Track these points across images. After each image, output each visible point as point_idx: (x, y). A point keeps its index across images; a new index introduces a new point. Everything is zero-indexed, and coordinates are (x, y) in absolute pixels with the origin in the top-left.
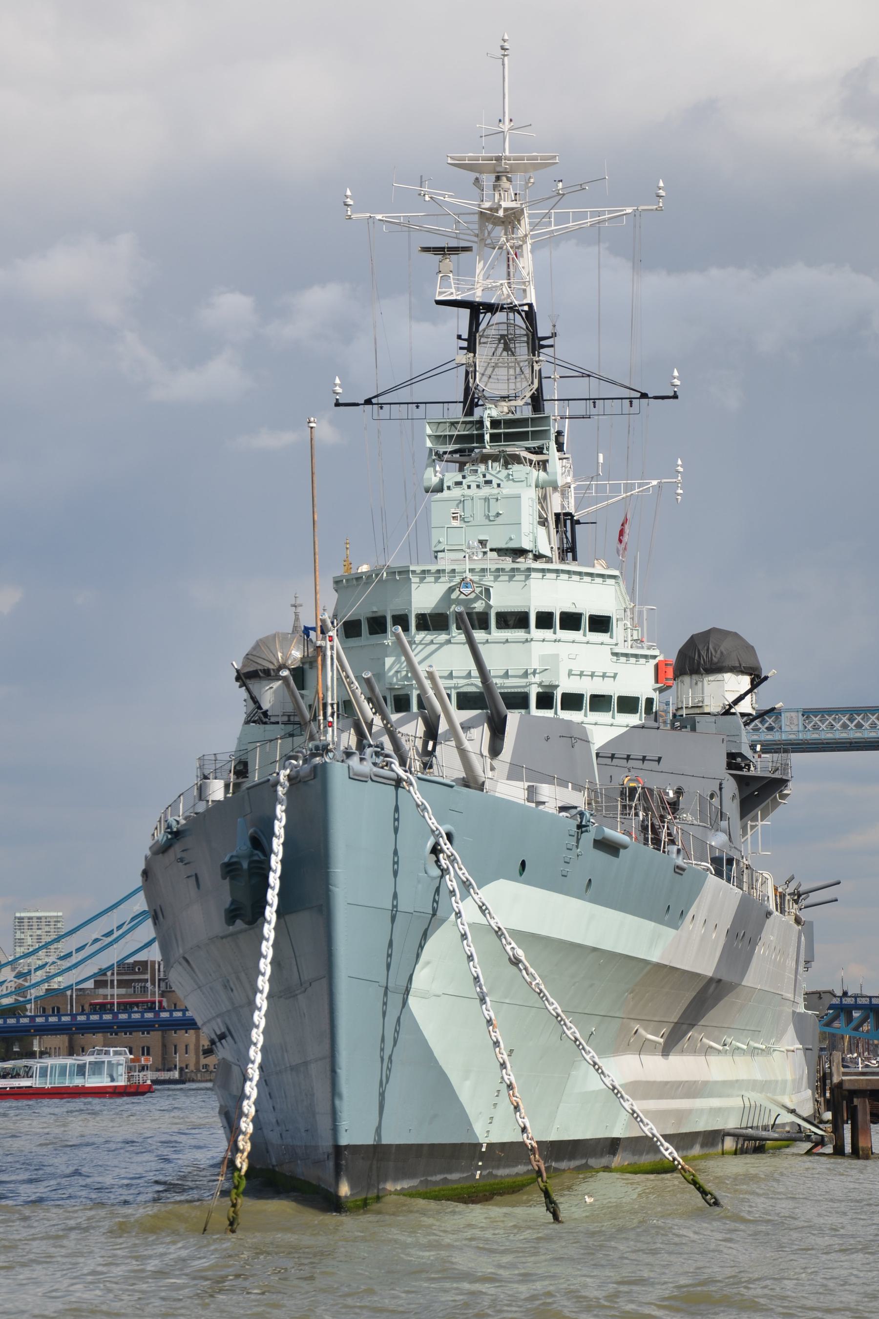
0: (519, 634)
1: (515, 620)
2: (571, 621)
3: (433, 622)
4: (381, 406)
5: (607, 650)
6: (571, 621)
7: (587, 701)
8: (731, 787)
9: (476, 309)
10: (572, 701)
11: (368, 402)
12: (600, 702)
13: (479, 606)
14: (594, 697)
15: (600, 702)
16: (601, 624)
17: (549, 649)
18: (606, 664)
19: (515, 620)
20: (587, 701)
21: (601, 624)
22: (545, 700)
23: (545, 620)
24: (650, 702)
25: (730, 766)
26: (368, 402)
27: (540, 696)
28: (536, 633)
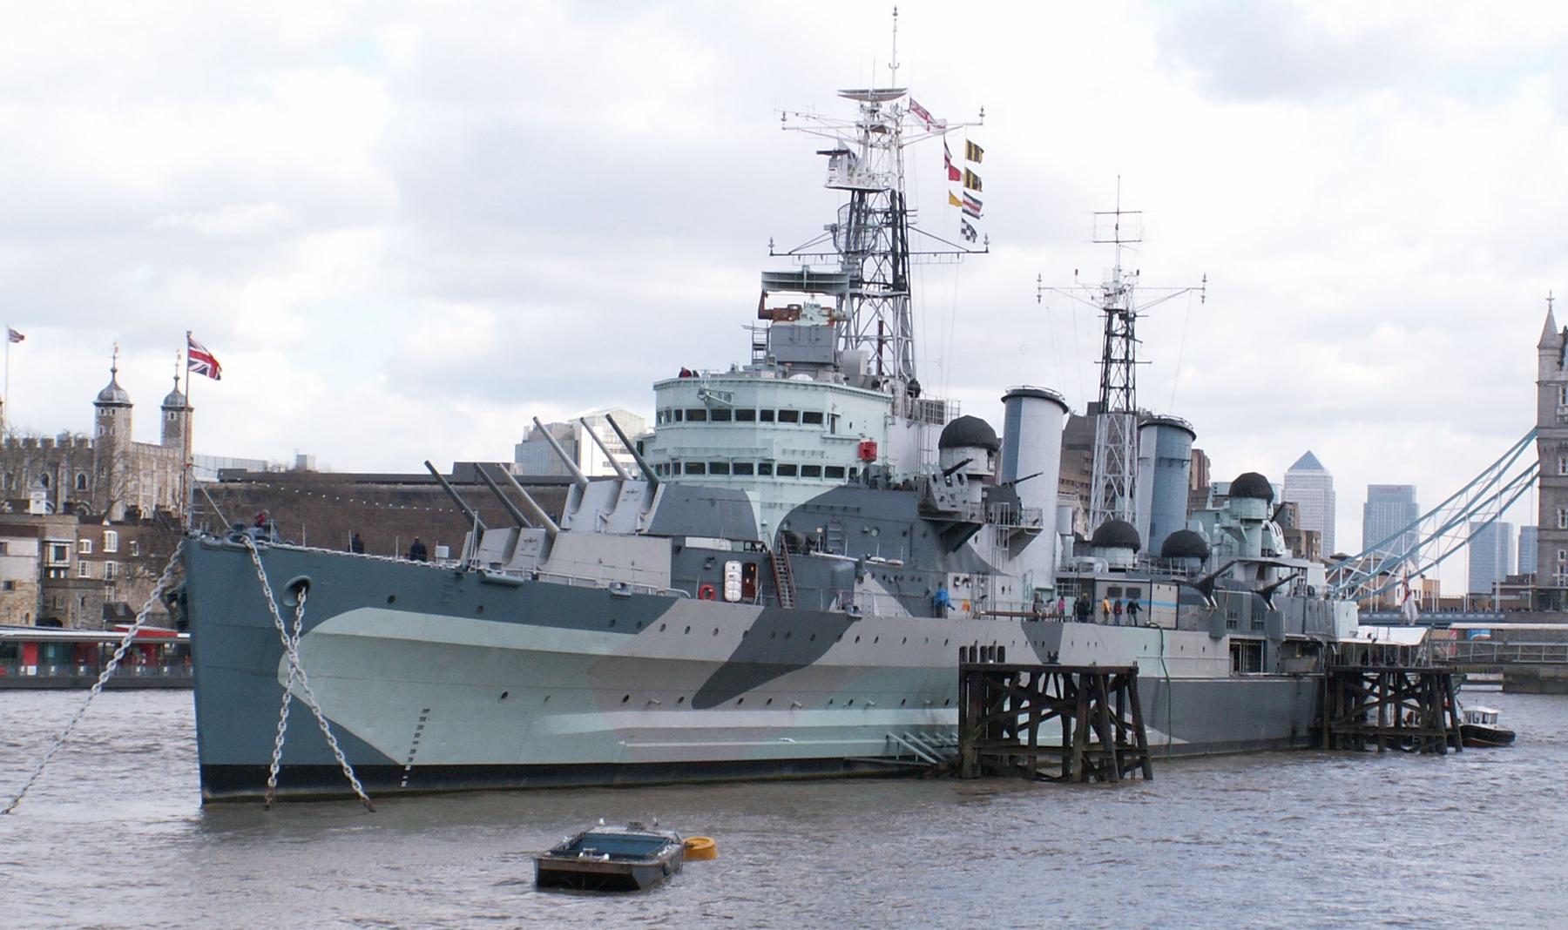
0: (749, 424)
1: (746, 415)
2: (788, 416)
3: (695, 415)
5: (816, 438)
6: (788, 416)
7: (799, 470)
8: (921, 527)
9: (862, 192)
10: (787, 470)
12: (811, 471)
15: (811, 471)
16: (813, 418)
17: (769, 436)
18: (817, 446)
19: (746, 415)
20: (799, 470)
21: (813, 418)
22: (765, 469)
23: (767, 416)
24: (853, 470)
25: (921, 513)
27: (761, 466)
28: (759, 424)
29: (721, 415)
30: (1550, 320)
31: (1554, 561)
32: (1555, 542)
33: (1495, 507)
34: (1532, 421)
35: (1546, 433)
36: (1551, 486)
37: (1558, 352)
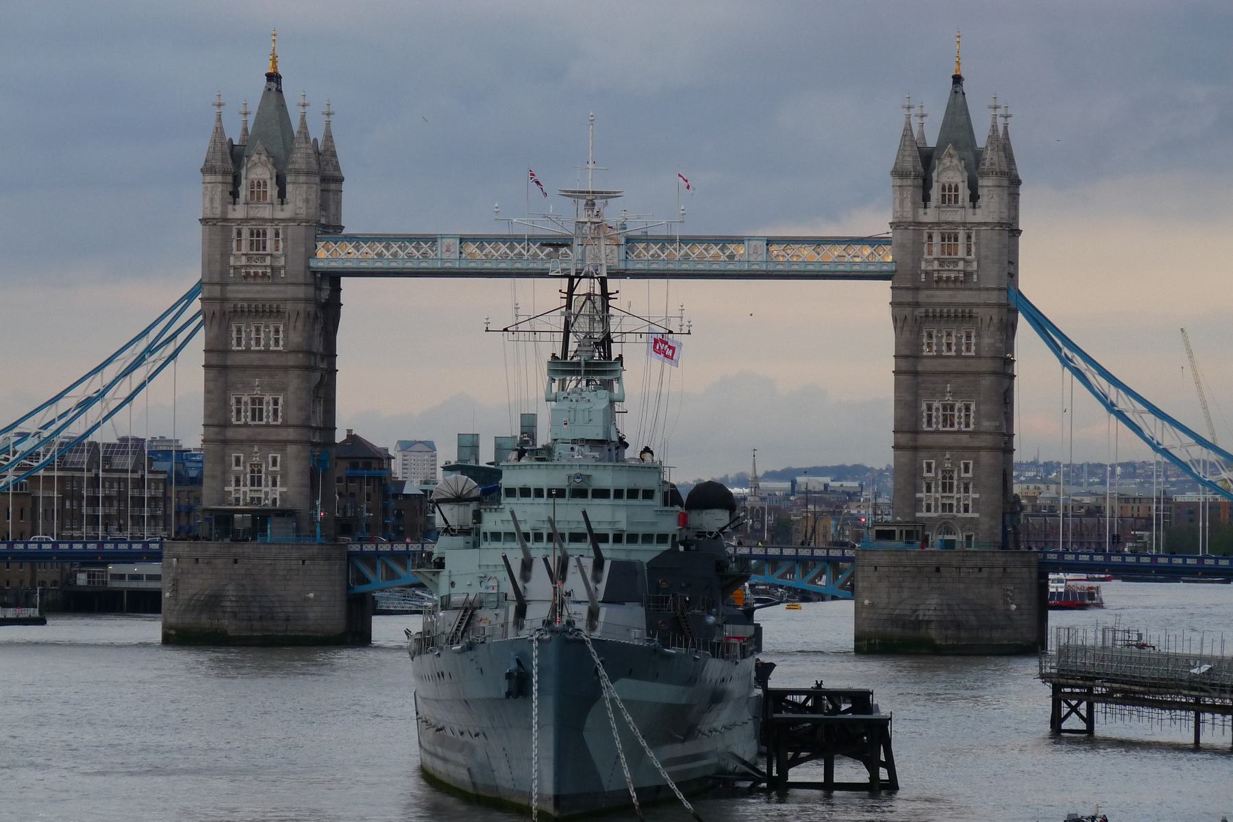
1: (601, 494)
2: (633, 494)
4: (513, 332)
6: (633, 494)
10: (632, 538)
11: (506, 330)
12: (647, 538)
13: (584, 486)
14: (644, 536)
15: (647, 538)
19: (601, 494)
22: (618, 538)
23: (619, 494)
24: (674, 536)
26: (506, 330)
27: (615, 536)
29: (580, 493)
30: (219, 131)
31: (225, 472)
32: (225, 442)
33: (124, 389)
34: (194, 275)
35: (216, 292)
36: (220, 365)
37: (230, 179)
